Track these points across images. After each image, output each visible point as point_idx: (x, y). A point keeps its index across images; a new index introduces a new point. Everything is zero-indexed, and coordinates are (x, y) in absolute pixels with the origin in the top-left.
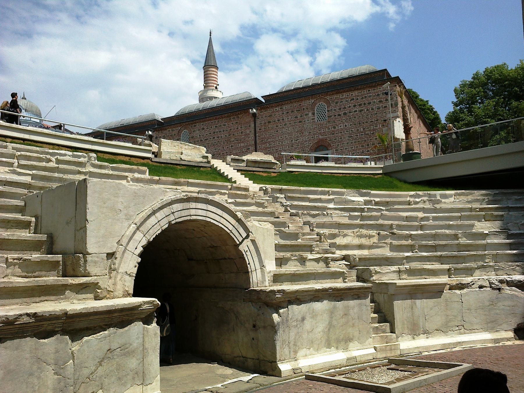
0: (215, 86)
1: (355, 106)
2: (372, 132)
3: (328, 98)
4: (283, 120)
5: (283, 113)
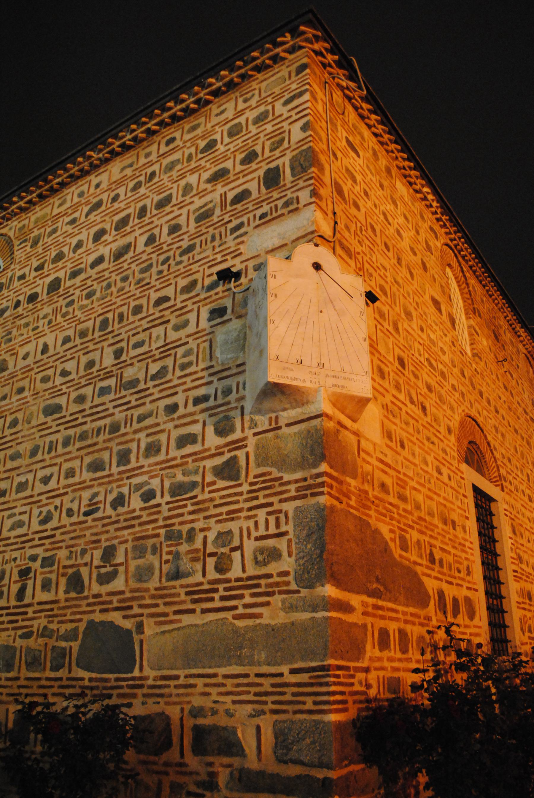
1: (98, 236)
2: (154, 368)
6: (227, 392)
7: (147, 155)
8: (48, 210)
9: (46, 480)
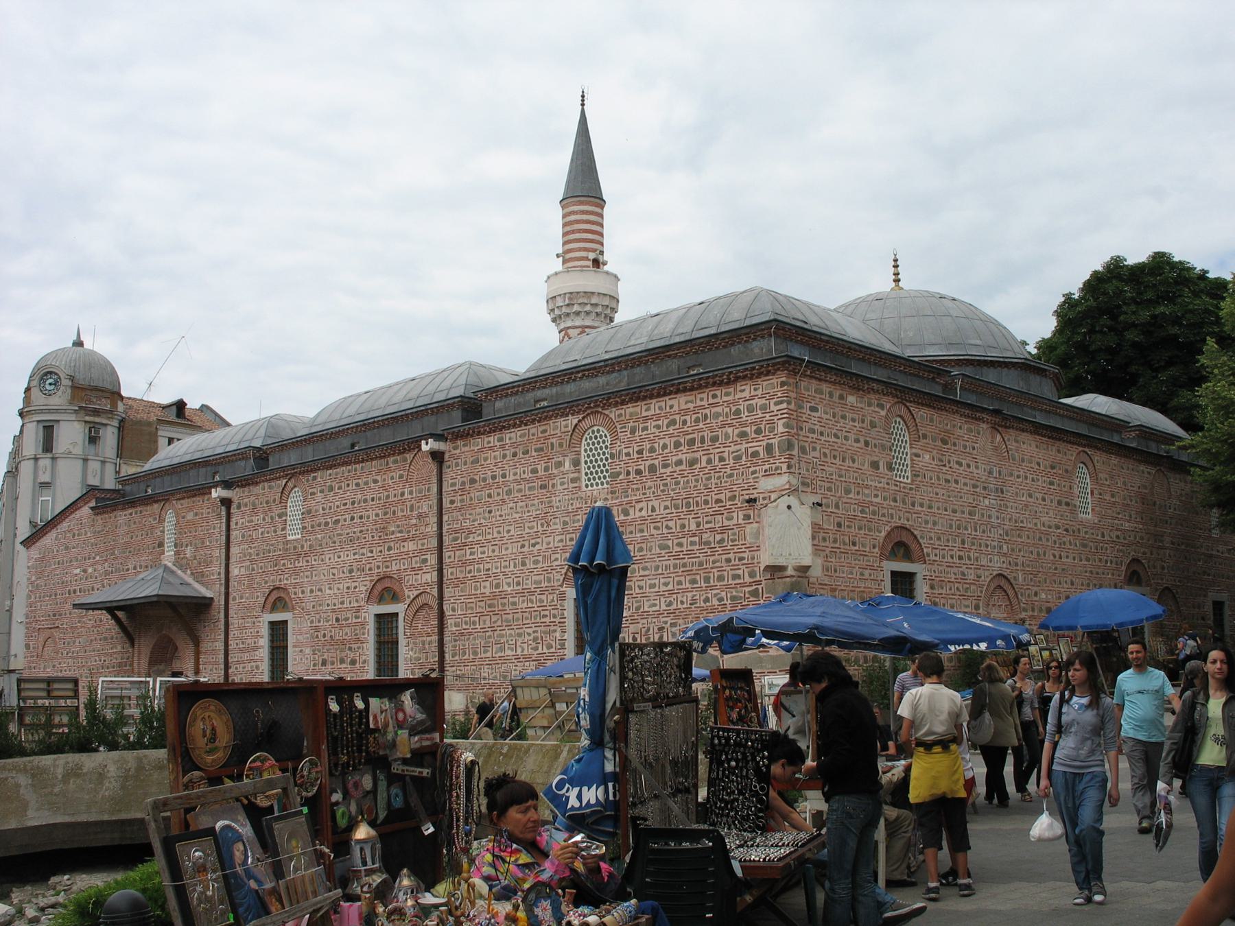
0: (592, 256)
2: (718, 537)
3: (613, 413)
4: (504, 476)
5: (505, 456)
6: (753, 558)
7: (702, 399)
8: (638, 409)
9: (666, 584)
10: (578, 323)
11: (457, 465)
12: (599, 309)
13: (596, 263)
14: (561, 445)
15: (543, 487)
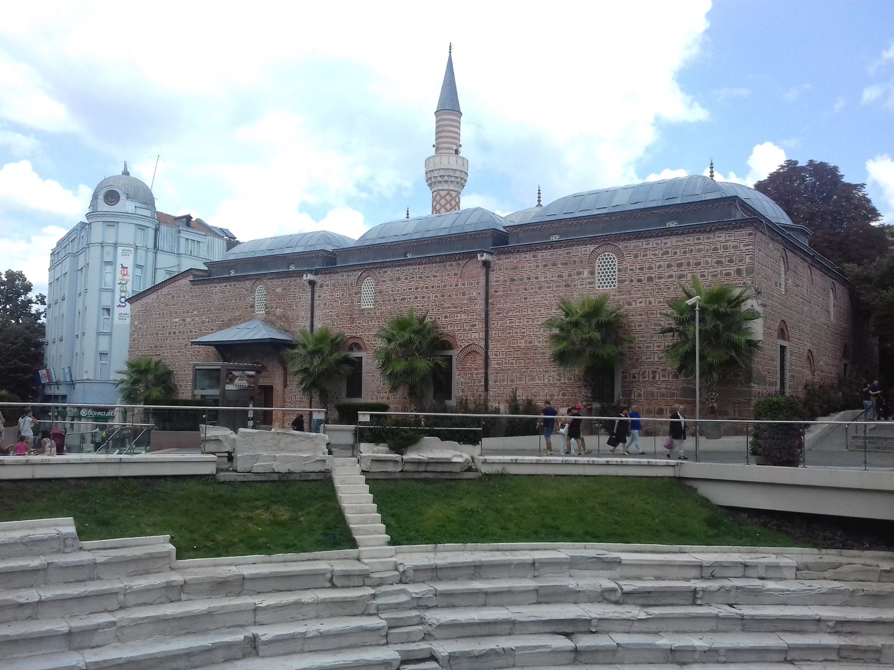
0: (455, 147)
1: (669, 266)
3: (621, 245)
5: (537, 266)
8: (640, 244)
9: (659, 347)
10: (446, 187)
11: (500, 269)
12: (459, 180)
13: (457, 152)
14: (581, 262)
15: (566, 286)
